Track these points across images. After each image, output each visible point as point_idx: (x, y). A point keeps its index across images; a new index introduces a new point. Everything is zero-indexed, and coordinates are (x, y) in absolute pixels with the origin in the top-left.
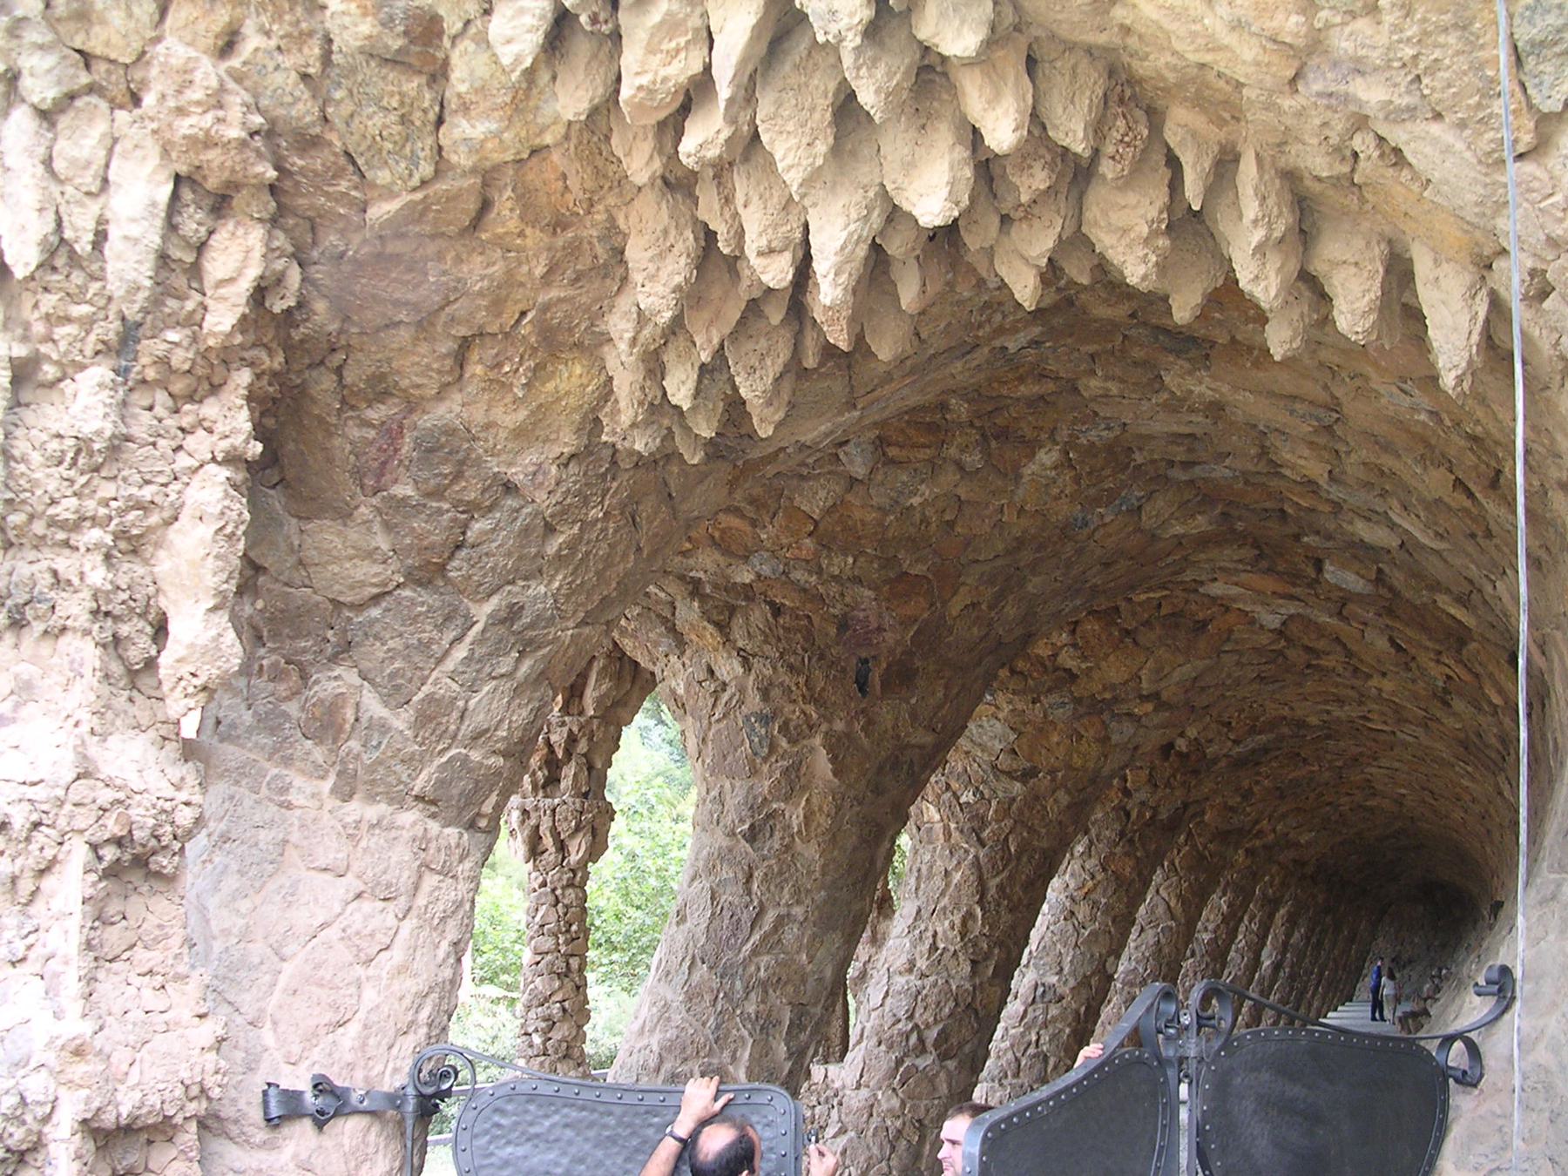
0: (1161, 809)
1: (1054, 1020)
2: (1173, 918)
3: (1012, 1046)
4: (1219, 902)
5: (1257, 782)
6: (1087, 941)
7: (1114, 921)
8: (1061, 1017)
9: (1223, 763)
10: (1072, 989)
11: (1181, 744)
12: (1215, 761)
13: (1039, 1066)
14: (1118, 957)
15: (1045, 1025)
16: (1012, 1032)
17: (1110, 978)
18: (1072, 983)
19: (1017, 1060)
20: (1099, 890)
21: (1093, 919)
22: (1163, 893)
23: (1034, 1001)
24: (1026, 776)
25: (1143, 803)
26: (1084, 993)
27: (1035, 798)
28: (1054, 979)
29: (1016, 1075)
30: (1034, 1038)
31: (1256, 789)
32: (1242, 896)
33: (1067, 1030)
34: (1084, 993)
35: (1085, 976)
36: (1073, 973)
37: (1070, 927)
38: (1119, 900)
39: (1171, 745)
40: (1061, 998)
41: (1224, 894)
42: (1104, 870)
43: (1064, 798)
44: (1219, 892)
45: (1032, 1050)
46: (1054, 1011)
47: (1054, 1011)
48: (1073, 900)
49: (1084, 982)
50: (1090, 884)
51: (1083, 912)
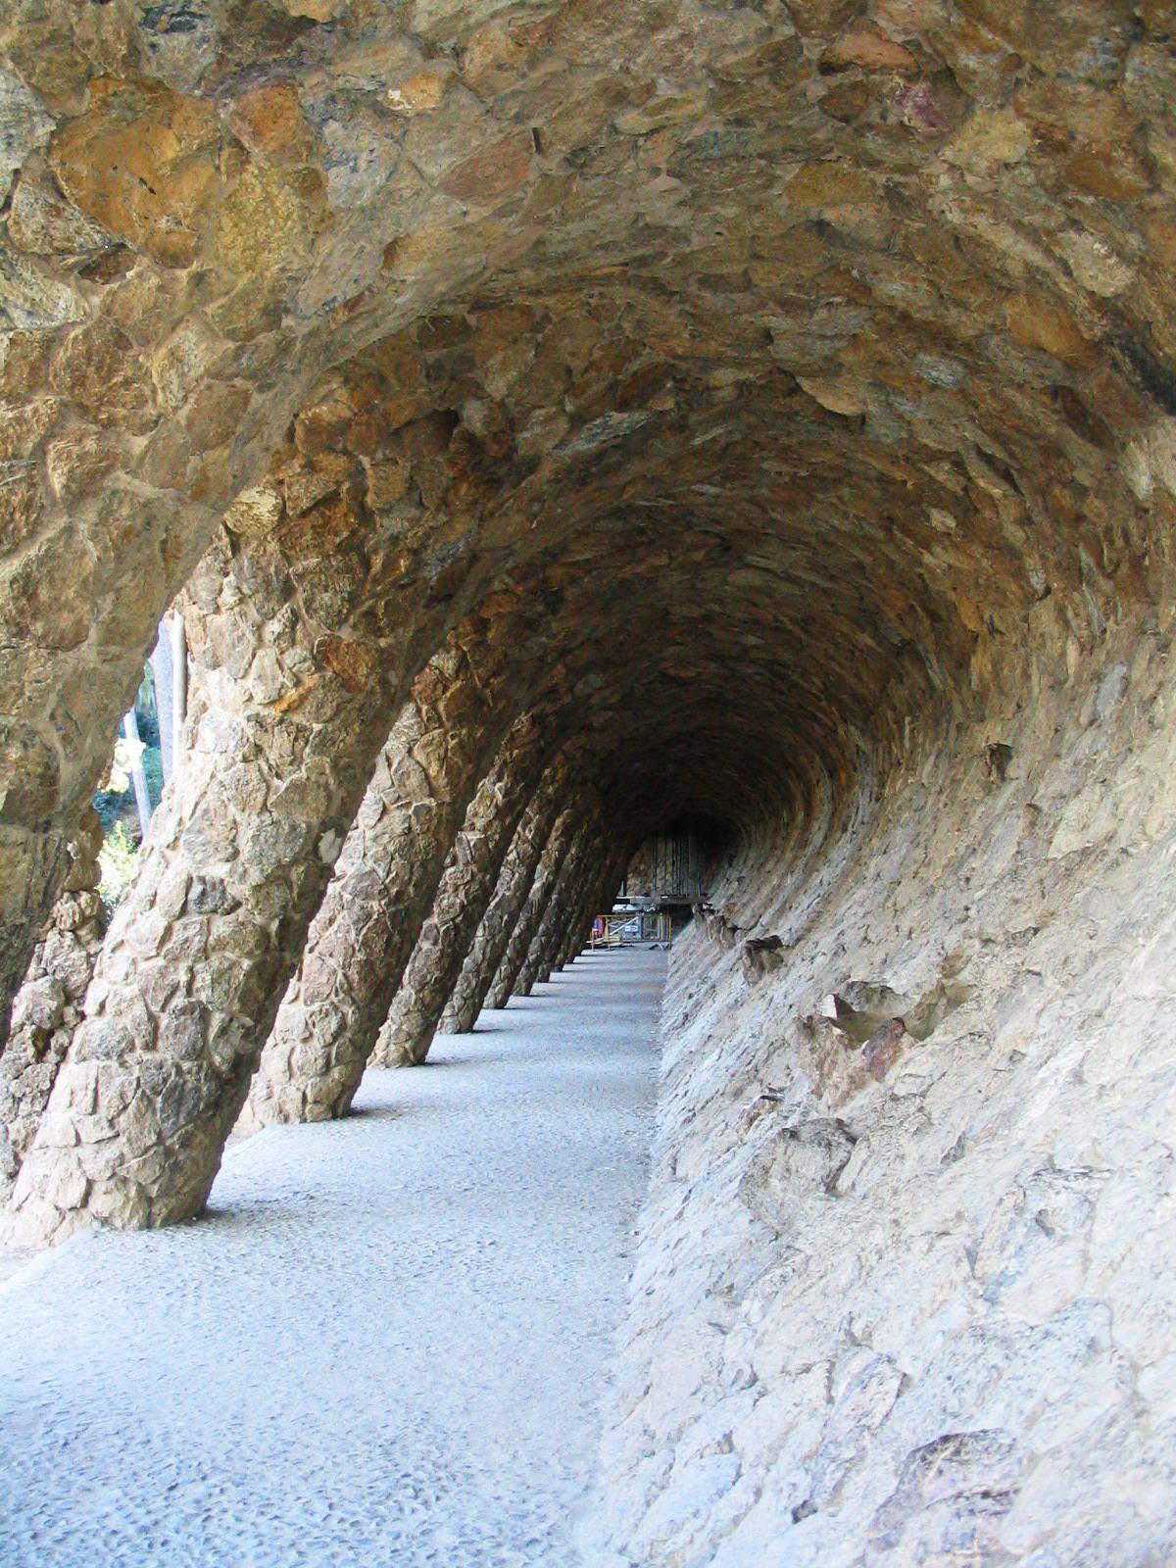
0: (429, 555)
1: (221, 945)
2: (432, 793)
3: (144, 992)
4: (493, 789)
5: (573, 581)
6: (284, 802)
7: (335, 766)
8: (235, 940)
9: (545, 472)
10: (257, 888)
11: (474, 416)
12: (533, 465)
13: (192, 1029)
14: (342, 833)
15: (205, 953)
16: (143, 966)
17: (326, 873)
18: (255, 877)
19: (152, 1018)
20: (308, 707)
21: (296, 760)
22: (419, 755)
23: (184, 911)
24: (100, 267)
25: (394, 540)
26: (278, 895)
27: (117, 340)
28: (218, 870)
29: (151, 1045)
30: (183, 977)
31: (571, 593)
32: (526, 779)
33: (246, 964)
34: (278, 895)
35: (280, 865)
37: (254, 775)
38: (346, 726)
39: (450, 419)
41: (499, 779)
42: (319, 668)
43: (196, 349)
44: (491, 778)
45: (179, 1001)
46: (221, 927)
48: (259, 722)
50: (292, 694)
51: (278, 746)
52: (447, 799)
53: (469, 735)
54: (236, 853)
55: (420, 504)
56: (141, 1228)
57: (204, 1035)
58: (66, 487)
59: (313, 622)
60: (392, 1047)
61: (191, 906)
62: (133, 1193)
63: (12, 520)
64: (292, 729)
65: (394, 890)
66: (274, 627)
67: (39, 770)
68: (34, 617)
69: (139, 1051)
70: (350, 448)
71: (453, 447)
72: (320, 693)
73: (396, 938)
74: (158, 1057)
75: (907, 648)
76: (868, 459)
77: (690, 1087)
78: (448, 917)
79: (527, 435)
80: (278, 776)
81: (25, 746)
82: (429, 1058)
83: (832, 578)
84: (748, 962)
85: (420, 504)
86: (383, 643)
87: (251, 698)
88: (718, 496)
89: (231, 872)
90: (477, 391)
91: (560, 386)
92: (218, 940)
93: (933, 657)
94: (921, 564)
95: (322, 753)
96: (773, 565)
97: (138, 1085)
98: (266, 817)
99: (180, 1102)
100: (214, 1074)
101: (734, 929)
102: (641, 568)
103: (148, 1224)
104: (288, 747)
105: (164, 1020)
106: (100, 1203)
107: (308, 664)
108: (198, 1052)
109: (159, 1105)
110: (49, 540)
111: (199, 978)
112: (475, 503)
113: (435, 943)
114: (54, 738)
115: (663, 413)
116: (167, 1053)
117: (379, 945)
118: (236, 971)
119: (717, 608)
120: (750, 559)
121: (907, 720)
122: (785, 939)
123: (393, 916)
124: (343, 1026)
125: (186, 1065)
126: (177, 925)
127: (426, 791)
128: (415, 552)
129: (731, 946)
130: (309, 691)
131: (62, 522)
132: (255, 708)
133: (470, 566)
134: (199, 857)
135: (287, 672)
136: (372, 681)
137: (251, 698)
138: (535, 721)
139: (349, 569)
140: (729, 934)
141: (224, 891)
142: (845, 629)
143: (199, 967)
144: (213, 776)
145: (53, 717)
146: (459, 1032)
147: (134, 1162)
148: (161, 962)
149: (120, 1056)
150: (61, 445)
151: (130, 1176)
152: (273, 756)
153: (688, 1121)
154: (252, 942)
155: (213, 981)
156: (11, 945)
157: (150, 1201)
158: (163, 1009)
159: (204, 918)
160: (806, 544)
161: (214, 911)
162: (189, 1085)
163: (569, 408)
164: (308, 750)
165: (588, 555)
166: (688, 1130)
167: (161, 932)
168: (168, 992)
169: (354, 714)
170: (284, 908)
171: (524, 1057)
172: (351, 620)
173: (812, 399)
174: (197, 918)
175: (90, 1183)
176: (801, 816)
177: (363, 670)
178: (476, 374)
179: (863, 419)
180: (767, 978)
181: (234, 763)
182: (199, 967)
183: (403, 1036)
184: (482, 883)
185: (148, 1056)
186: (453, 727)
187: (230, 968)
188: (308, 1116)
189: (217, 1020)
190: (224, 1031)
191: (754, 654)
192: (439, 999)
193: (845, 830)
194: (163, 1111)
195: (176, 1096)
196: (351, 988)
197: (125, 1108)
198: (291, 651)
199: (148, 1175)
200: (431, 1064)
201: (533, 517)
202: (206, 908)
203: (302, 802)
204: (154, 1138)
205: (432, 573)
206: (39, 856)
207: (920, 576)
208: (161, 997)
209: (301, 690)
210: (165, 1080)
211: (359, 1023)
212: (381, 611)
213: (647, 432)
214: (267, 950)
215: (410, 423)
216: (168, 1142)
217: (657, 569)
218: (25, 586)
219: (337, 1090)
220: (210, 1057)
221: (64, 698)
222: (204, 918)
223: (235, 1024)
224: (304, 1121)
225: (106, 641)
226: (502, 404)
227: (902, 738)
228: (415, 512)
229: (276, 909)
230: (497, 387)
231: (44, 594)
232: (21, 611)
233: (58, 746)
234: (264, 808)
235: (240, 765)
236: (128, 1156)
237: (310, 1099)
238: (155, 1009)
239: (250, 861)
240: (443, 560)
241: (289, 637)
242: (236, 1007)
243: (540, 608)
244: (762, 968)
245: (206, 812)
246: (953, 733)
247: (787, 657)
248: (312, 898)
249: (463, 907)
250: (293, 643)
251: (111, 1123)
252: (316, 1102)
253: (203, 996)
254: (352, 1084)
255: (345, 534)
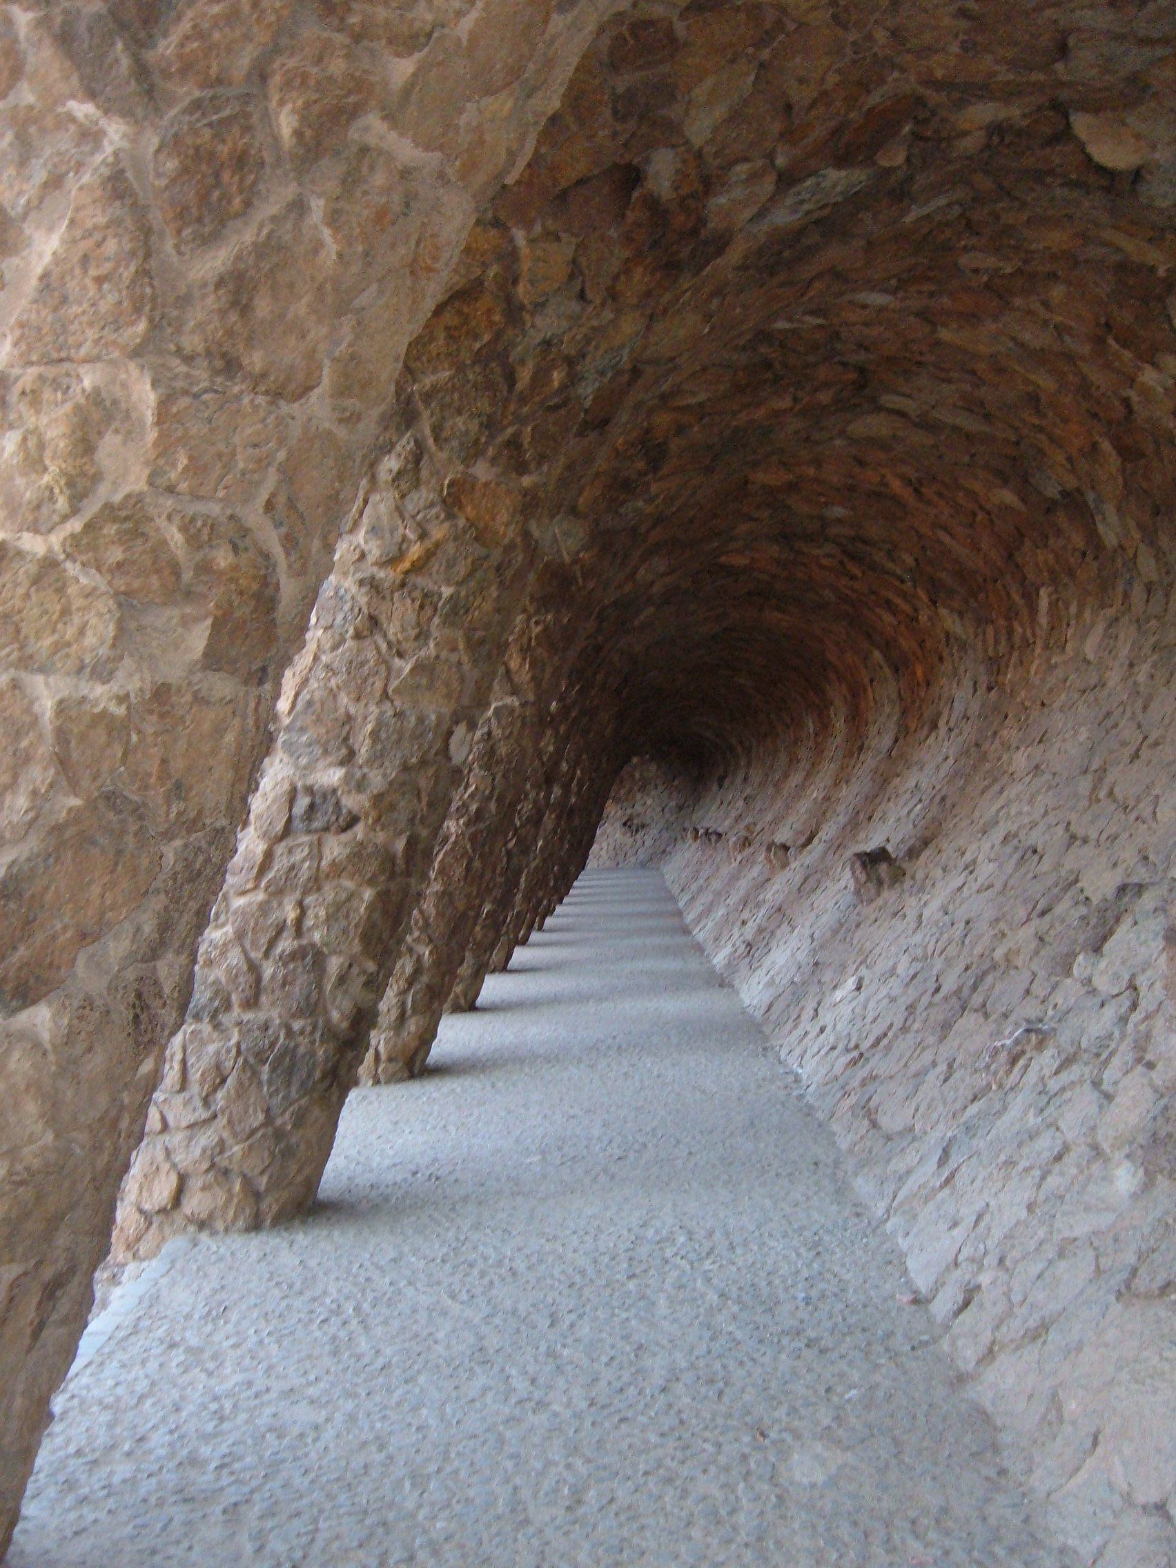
0: (588, 367)
1: (337, 869)
2: (515, 691)
3: (240, 935)
9: (735, 254)
10: (378, 799)
11: (663, 171)
12: (721, 243)
13: (303, 979)
15: (315, 883)
18: (377, 780)
19: (254, 968)
20: (436, 566)
21: (422, 635)
23: (287, 831)
28: (331, 776)
29: (251, 1003)
30: (291, 914)
31: (675, 444)
33: (368, 894)
36: (377, 758)
37: (371, 654)
40: (353, 821)
42: (450, 516)
45: (286, 944)
46: (335, 848)
47: (335, 848)
49: (405, 782)
50: (415, 551)
51: (399, 618)
52: (531, 697)
53: (557, 620)
54: (352, 754)
55: (582, 296)
56: (248, 1230)
57: (320, 987)
58: (298, 133)
59: (443, 455)
61: (297, 824)
62: (237, 1187)
63: (218, 184)
64: (417, 594)
65: (474, 807)
66: (391, 464)
67: (255, 586)
68: (250, 341)
69: (236, 1010)
70: (502, 215)
71: (631, 216)
72: (451, 548)
73: (477, 864)
74: (262, 1016)
75: (1074, 503)
76: (1120, 240)
77: (826, 1017)
79: (722, 200)
80: (400, 655)
81: (235, 548)
82: (479, 1001)
83: (987, 417)
84: (863, 878)
85: (582, 296)
86: (527, 481)
87: (363, 556)
88: (882, 309)
89: (347, 779)
90: (671, 132)
91: (776, 127)
92: (333, 864)
93: (1110, 510)
94: (1132, 381)
95: (453, 624)
96: (910, 406)
97: (239, 1052)
98: (387, 706)
99: (290, 1072)
100: (330, 1032)
101: (785, 848)
102: (759, 414)
103: (255, 1226)
104: (411, 617)
105: (268, 970)
106: (195, 1203)
107: (434, 511)
108: (311, 1008)
109: (265, 1077)
110: (274, 219)
111: (310, 913)
112: (648, 294)
114: (272, 539)
115: (888, 171)
116: (271, 1012)
117: (458, 871)
118: (355, 903)
119: (811, 471)
120: (888, 400)
121: (1043, 592)
122: (890, 848)
123: (473, 838)
124: (418, 971)
125: (297, 1025)
126: (280, 849)
127: (508, 688)
128: (570, 362)
129: (785, 865)
130: (437, 545)
131: (290, 191)
132: (369, 569)
133: (630, 384)
134: (304, 761)
135: (410, 522)
136: (511, 533)
137: (363, 556)
139: (490, 386)
140: (781, 853)
141: (338, 803)
142: (977, 486)
143: (309, 900)
144: (316, 658)
145: (269, 506)
147: (236, 1148)
148: (260, 896)
149: (213, 1017)
150: (292, 63)
151: (235, 1167)
152: (393, 630)
153: (854, 1062)
154: (372, 867)
155: (329, 917)
156: (208, 860)
157: (258, 1196)
158: (267, 954)
159: (315, 837)
160: (973, 373)
161: (326, 829)
162: (302, 1050)
163: (781, 161)
164: (436, 620)
165: (702, 397)
166: (862, 1073)
167: (259, 858)
168: (271, 933)
169: (491, 575)
170: (412, 821)
171: (581, 998)
172: (491, 452)
173: (1081, 147)
174: (305, 839)
175: (183, 1179)
176: (840, 725)
177: (504, 516)
178: (674, 112)
179: (1137, 175)
180: (886, 893)
181: (342, 641)
182: (309, 900)
184: (535, 802)
185: (248, 1016)
186: (537, 612)
187: (349, 899)
188: (382, 1077)
189: (334, 964)
190: (342, 979)
191: (834, 531)
192: (491, 935)
193: (934, 726)
194: (270, 1082)
195: (286, 1064)
196: (427, 924)
197: (224, 1081)
198: (415, 495)
199: (254, 1165)
200: (484, 1010)
201: (707, 317)
202: (317, 824)
203: (430, 687)
204: (261, 1117)
205: (587, 391)
206: (250, 721)
207: (1126, 402)
208: (264, 941)
209: (428, 544)
210: (272, 1045)
211: (437, 964)
212: (526, 441)
213: (856, 202)
214: (392, 876)
215: (581, 182)
216: (279, 1122)
217: (776, 413)
218: (237, 292)
219: (414, 1044)
220: (326, 1012)
221: (288, 475)
222: (315, 837)
223: (355, 970)
224: (377, 1082)
225: (341, 391)
226: (699, 155)
227: (1033, 610)
228: (575, 306)
229: (403, 824)
230: (701, 127)
231: (263, 307)
232: (230, 333)
233: (278, 551)
234: (385, 695)
235: (349, 643)
236: (230, 1141)
237: (383, 1056)
238: (256, 955)
239: (370, 762)
240: (602, 373)
241: (409, 476)
242: (357, 947)
243: (641, 465)
244: (880, 883)
245: (310, 703)
246: (1138, 592)
247: (874, 530)
248: (439, 805)
250: (416, 484)
251: (206, 1102)
252: (390, 1060)
253: (317, 937)
254: (428, 1036)
255: (486, 338)
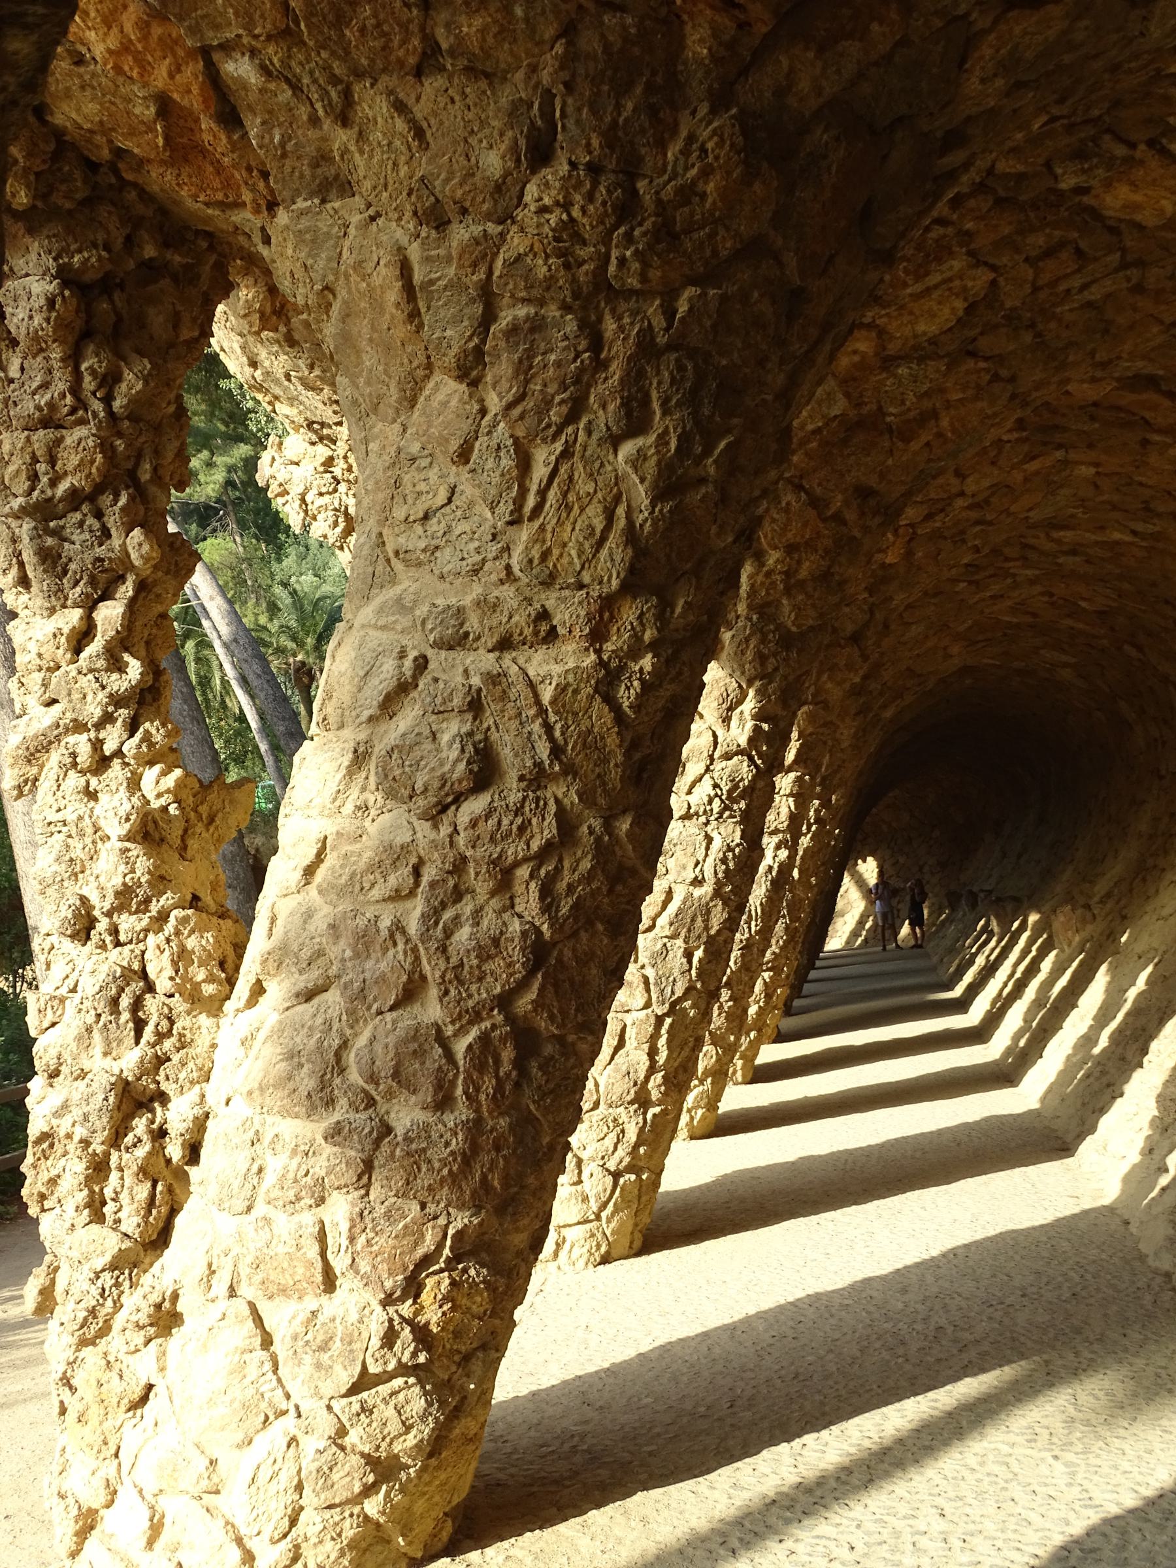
41: (635, 421)
60: (311, 1523)
78: (480, 994)
113: (443, 1102)
138: (768, 144)
146: (605, 1260)
183: (350, 1475)
184: (602, 852)
249: (538, 952)
